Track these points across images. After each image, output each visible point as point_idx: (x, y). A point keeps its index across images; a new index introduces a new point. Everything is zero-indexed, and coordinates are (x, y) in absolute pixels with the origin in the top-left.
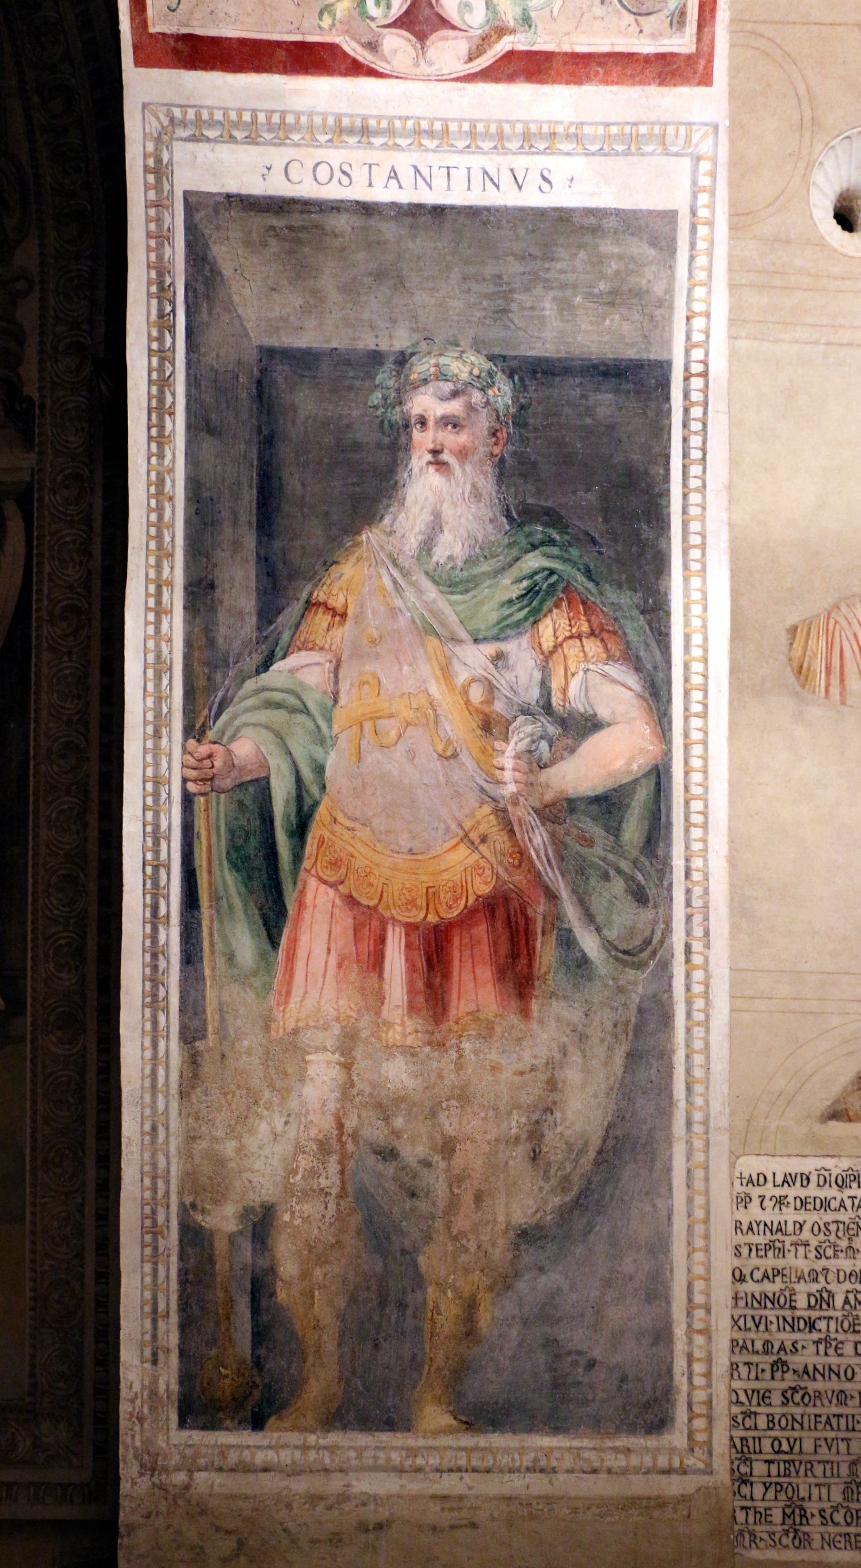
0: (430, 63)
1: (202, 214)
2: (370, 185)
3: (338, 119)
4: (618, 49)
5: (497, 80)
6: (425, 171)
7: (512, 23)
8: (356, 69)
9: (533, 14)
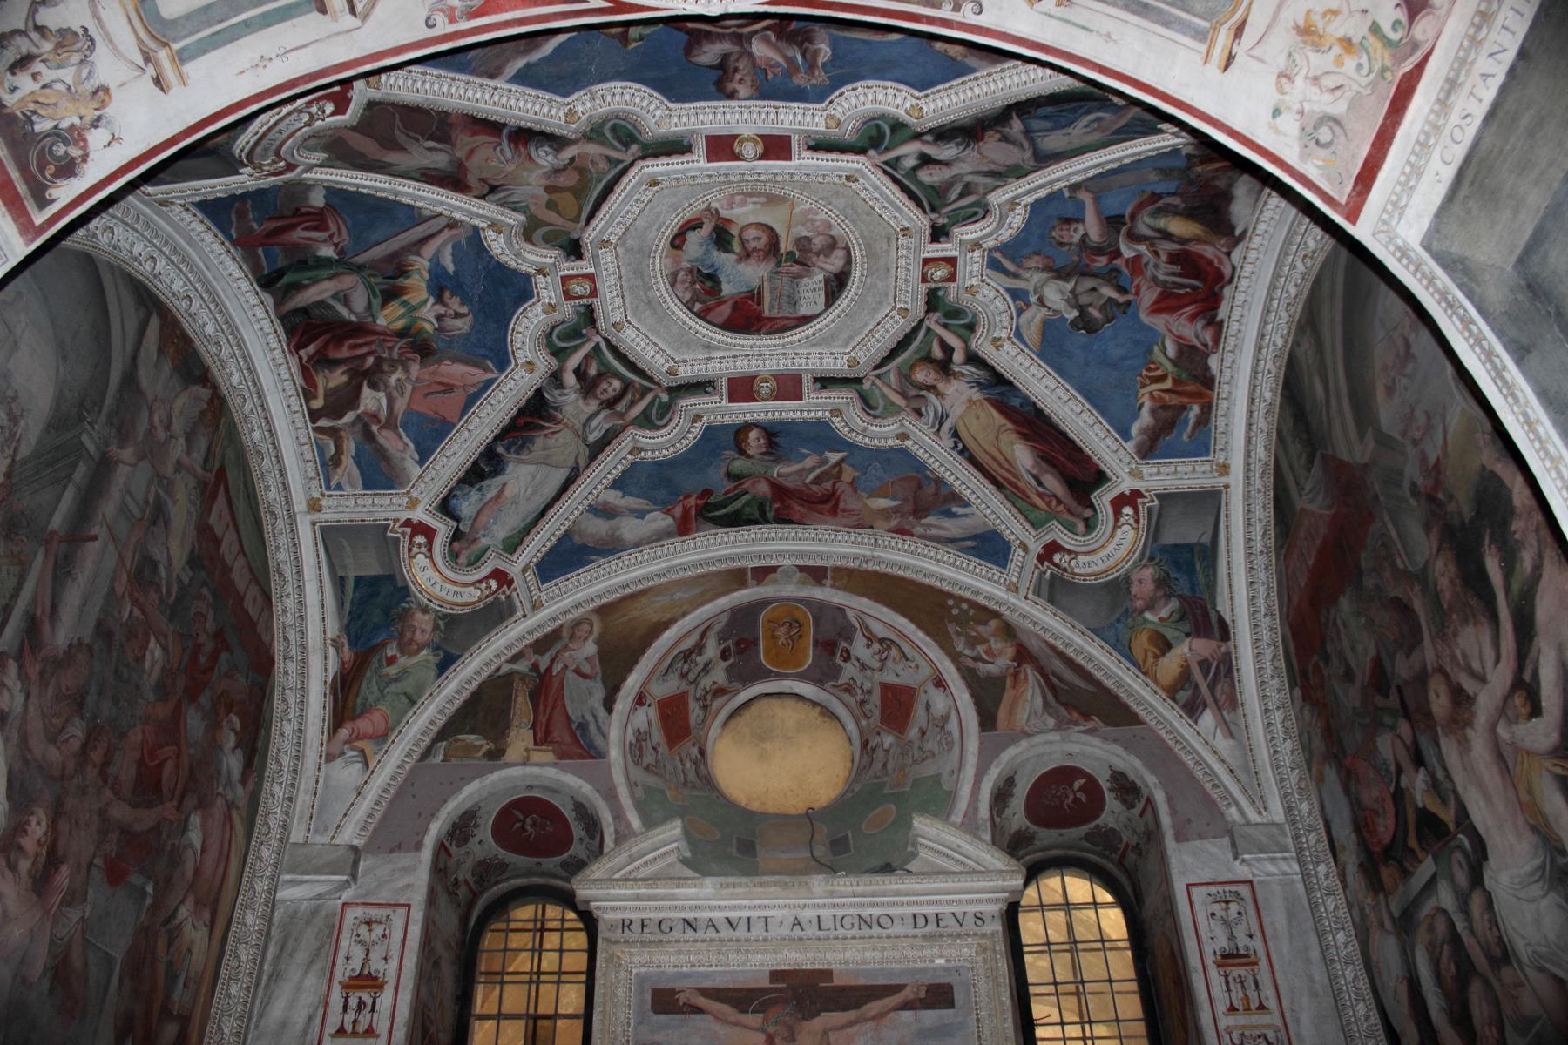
1: (1435, 243)
3: (1438, 100)
6: (1496, 48)
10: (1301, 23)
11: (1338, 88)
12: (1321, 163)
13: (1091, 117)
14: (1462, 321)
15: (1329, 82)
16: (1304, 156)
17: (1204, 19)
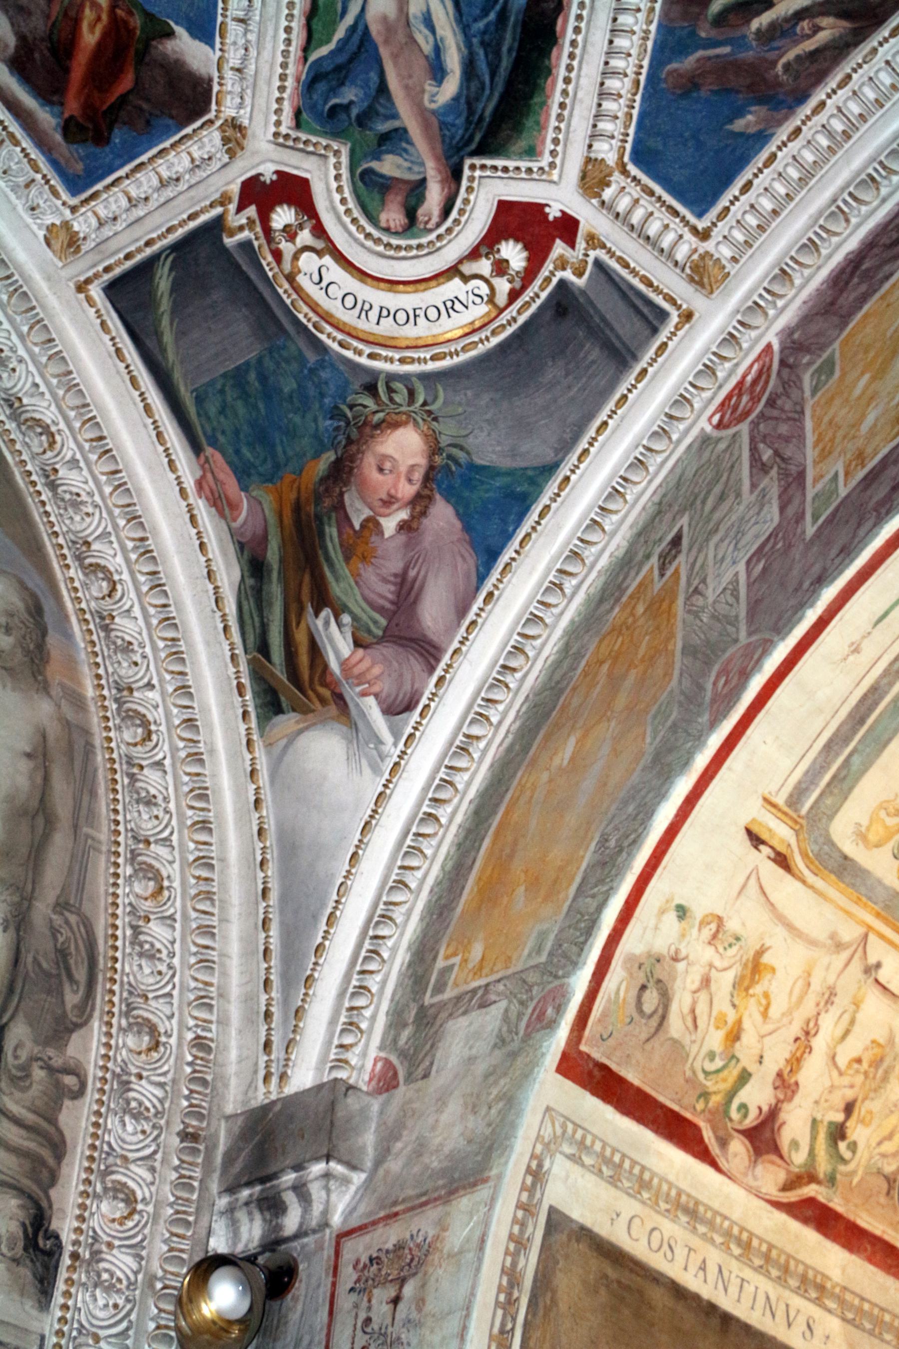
0: (755, 1178)
2: (686, 1269)
4: (886, 1237)
5: (795, 1217)
7: (821, 1176)
8: (704, 1155)
9: (838, 1177)
10: (766, 959)
11: (695, 1020)
12: (622, 994)
13: (453, 61)
14: (502, 1331)
15: (702, 1009)
16: (630, 959)
17: (812, 808)
